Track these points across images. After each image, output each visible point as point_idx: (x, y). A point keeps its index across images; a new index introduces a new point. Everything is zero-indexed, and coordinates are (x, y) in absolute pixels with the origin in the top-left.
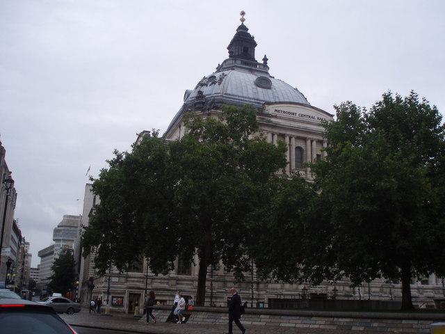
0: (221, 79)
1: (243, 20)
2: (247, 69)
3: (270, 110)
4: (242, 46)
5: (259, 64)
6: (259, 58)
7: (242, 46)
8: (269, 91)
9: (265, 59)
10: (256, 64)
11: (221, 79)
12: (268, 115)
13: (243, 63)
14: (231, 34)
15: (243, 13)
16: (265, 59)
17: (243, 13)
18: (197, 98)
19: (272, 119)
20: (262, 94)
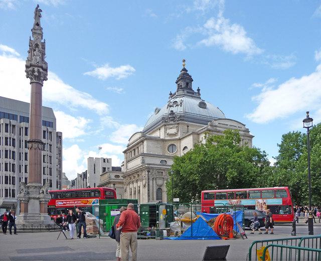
0: (181, 103)
1: (184, 65)
2: (191, 96)
3: (216, 123)
4: (185, 82)
5: (196, 93)
6: (195, 89)
7: (185, 82)
8: (206, 110)
9: (199, 90)
10: (193, 93)
11: (181, 103)
12: (216, 126)
13: (188, 92)
14: (178, 73)
15: (184, 61)
16: (199, 90)
17: (184, 61)
18: (170, 114)
19: (218, 128)
20: (202, 111)
